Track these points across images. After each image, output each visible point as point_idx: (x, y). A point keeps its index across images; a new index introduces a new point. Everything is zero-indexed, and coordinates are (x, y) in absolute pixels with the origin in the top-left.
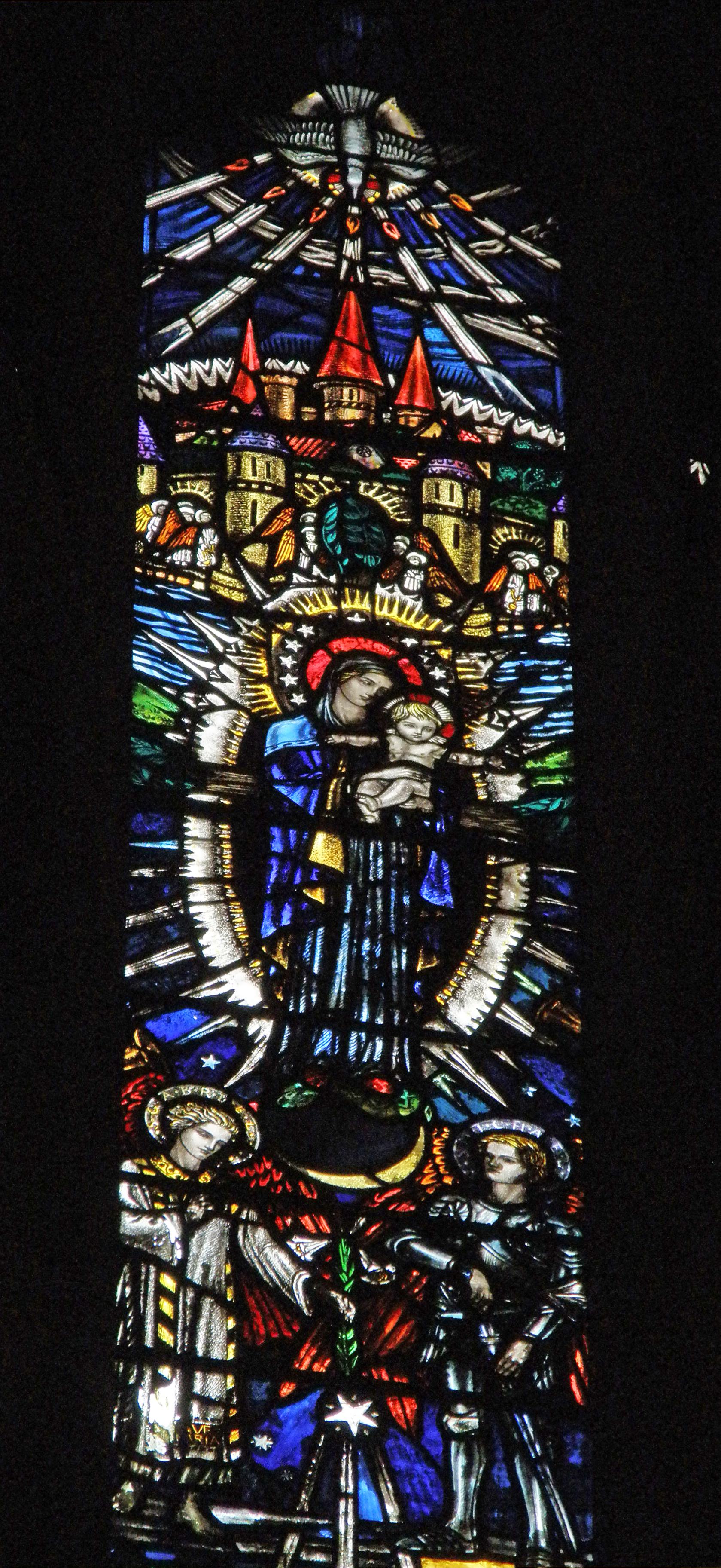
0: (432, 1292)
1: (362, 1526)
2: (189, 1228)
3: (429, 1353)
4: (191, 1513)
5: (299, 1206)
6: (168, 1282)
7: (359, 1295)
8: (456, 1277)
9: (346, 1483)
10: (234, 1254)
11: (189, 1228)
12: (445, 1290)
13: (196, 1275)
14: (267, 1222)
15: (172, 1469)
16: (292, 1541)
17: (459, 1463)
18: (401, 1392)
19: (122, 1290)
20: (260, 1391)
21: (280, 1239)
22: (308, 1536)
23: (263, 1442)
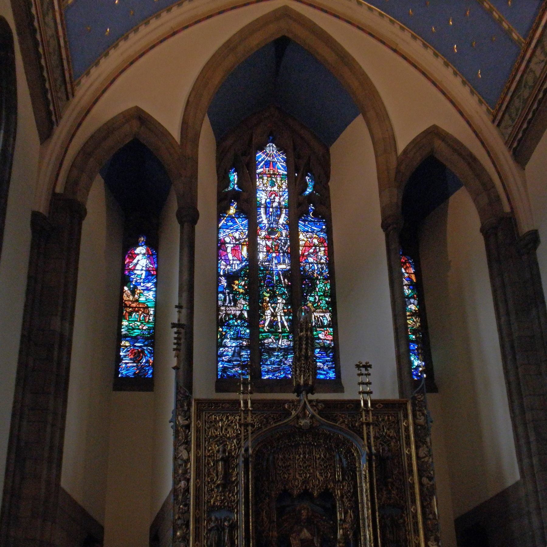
0: (279, 244)
1: (275, 263)
2: (263, 241)
3: (279, 249)
4: (263, 264)
5: (270, 239)
6: (261, 246)
7: (274, 245)
8: (281, 243)
9: (274, 260)
10: (266, 243)
11: (263, 241)
12: (280, 244)
13: (263, 245)
14: (268, 240)
15: (262, 260)
16: (270, 265)
17: (281, 257)
18: (277, 253)
19: (258, 247)
20: (268, 254)
21: (269, 241)
22: (271, 264)
23: (268, 258)
